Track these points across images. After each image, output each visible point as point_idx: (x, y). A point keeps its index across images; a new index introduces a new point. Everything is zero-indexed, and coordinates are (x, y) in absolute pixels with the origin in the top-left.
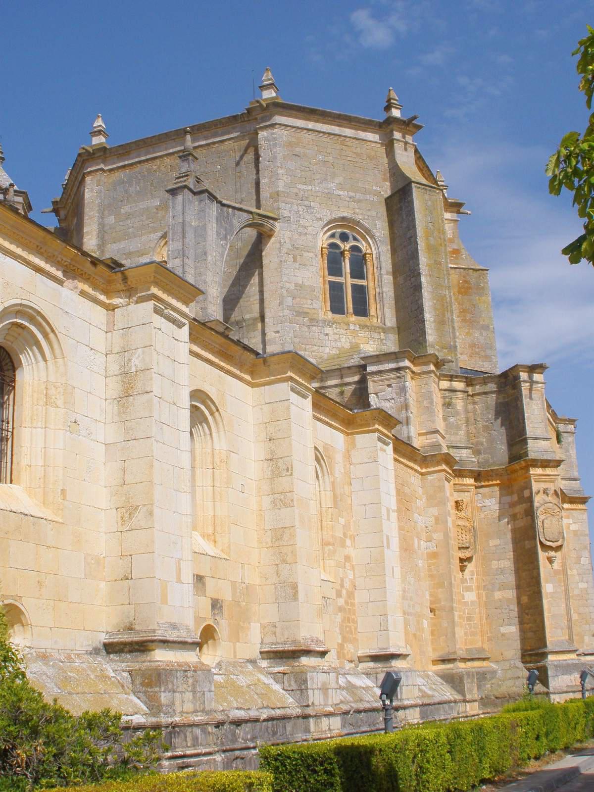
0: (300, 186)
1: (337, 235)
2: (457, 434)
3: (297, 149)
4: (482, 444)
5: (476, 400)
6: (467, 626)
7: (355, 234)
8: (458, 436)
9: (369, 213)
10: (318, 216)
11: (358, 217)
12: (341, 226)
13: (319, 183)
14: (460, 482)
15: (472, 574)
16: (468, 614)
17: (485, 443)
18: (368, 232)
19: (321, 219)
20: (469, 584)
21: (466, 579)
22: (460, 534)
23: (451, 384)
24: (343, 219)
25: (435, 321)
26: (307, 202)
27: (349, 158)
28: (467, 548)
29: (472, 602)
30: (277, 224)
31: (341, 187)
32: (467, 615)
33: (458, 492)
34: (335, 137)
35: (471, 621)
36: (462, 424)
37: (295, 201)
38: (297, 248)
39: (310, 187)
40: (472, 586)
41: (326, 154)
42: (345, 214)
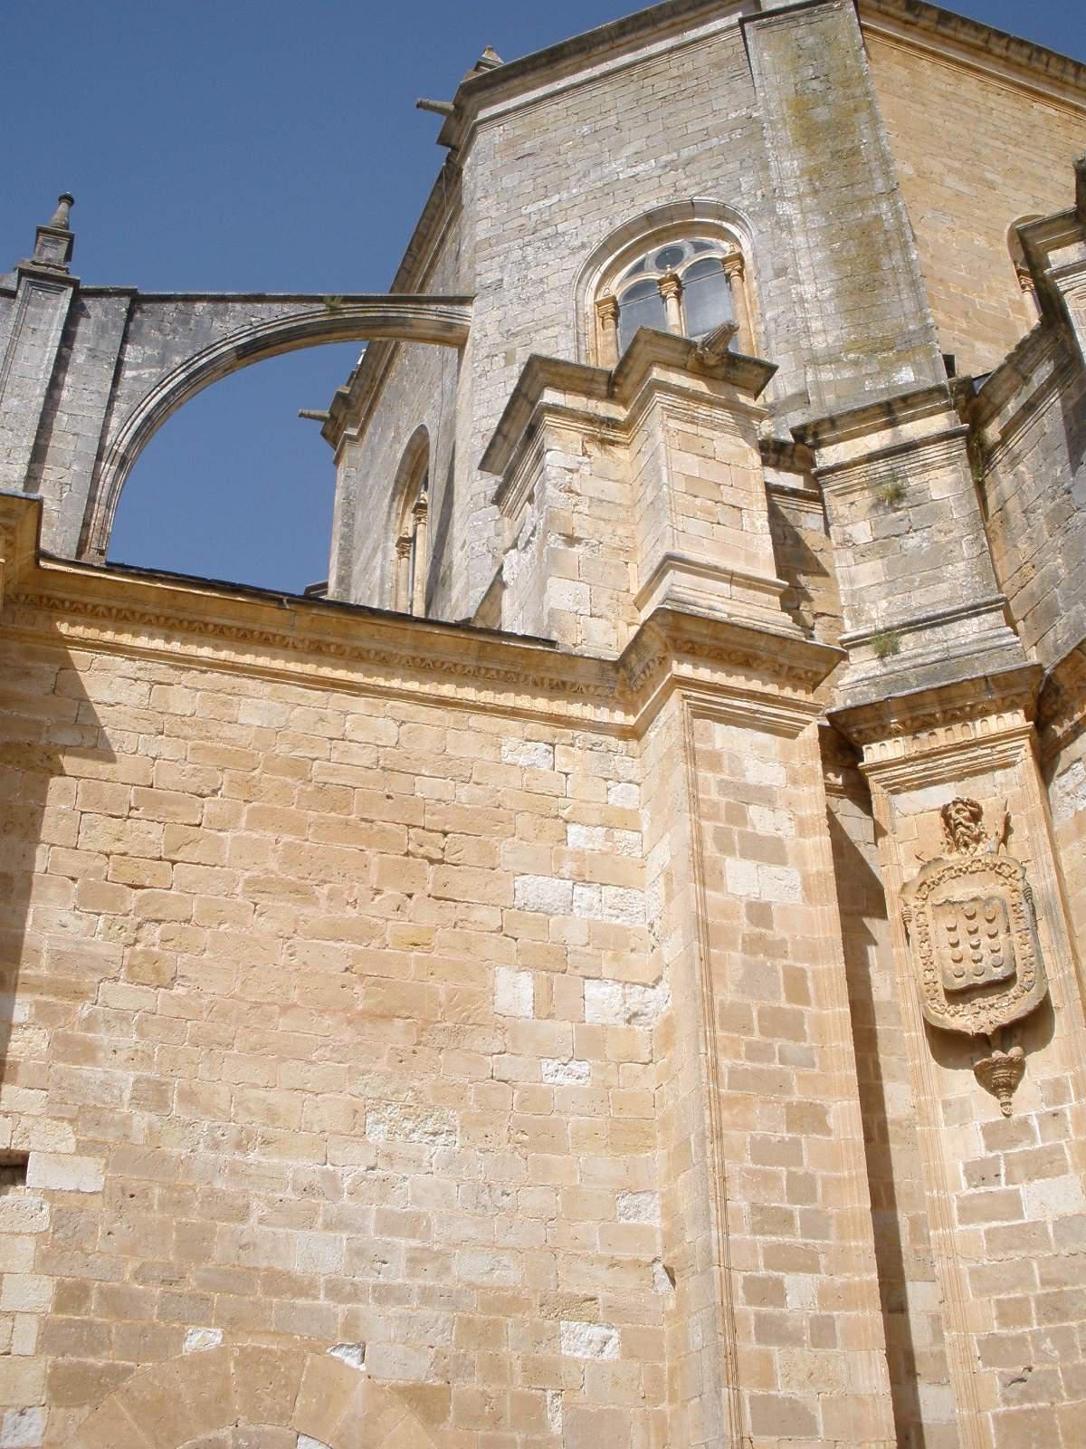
0: (531, 208)
1: (650, 263)
2: (940, 580)
3: (527, 145)
4: (1054, 580)
5: (1016, 449)
6: (1047, 1344)
7: (698, 239)
8: (945, 586)
9: (717, 173)
10: (577, 243)
11: (691, 193)
12: (657, 238)
13: (579, 180)
14: (960, 739)
15: (1056, 1091)
16: (1045, 1283)
17: (1062, 571)
18: (723, 212)
19: (583, 246)
20: (1039, 1145)
21: (1024, 1123)
22: (961, 934)
23: (895, 435)
24: (650, 218)
25: (838, 294)
26: (549, 230)
27: (661, 95)
28: (1008, 981)
29: (1063, 1223)
30: (469, 310)
31: (639, 156)
32: (1039, 1291)
33: (960, 778)
34: (623, 75)
35: (1064, 1315)
36: (958, 541)
37: (512, 244)
38: (515, 335)
39: (555, 198)
40: (1060, 1149)
41: (599, 118)
42: (653, 203)
